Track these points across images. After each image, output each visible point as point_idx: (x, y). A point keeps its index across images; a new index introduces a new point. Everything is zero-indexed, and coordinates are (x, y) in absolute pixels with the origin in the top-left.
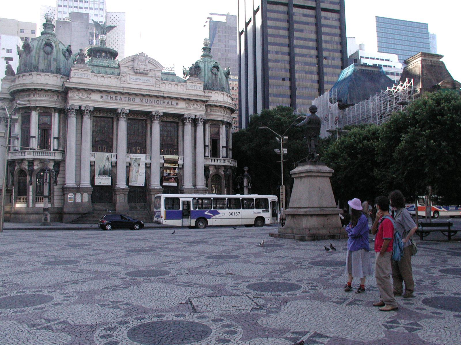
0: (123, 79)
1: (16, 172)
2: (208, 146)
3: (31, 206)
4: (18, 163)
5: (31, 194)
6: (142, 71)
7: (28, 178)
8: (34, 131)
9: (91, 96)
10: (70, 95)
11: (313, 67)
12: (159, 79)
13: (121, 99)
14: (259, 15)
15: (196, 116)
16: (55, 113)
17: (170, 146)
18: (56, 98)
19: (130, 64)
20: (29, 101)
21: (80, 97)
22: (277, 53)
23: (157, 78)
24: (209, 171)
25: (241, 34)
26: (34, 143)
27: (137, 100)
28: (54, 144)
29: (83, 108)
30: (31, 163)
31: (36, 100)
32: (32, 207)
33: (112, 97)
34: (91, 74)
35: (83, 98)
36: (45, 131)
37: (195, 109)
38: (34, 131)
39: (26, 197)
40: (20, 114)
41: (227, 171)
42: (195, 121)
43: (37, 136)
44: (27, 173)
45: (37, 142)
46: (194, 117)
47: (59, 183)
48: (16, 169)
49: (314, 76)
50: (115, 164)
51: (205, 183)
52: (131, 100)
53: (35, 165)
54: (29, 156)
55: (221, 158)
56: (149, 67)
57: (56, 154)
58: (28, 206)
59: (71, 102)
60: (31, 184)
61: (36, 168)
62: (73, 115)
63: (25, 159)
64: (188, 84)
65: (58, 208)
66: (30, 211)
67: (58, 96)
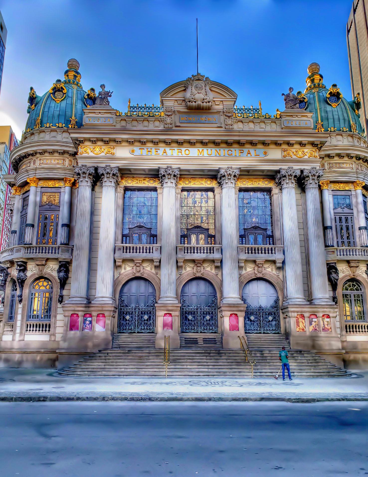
2: (331, 228)
5: (19, 317)
6: (199, 102)
9: (113, 151)
12: (230, 115)
15: (302, 171)
24: (336, 272)
29: (100, 171)
31: (36, 169)
33: (149, 150)
34: (114, 116)
45: (36, 233)
46: (298, 173)
50: (158, 264)
51: (331, 294)
59: (81, 162)
61: (29, 273)
62: (84, 183)
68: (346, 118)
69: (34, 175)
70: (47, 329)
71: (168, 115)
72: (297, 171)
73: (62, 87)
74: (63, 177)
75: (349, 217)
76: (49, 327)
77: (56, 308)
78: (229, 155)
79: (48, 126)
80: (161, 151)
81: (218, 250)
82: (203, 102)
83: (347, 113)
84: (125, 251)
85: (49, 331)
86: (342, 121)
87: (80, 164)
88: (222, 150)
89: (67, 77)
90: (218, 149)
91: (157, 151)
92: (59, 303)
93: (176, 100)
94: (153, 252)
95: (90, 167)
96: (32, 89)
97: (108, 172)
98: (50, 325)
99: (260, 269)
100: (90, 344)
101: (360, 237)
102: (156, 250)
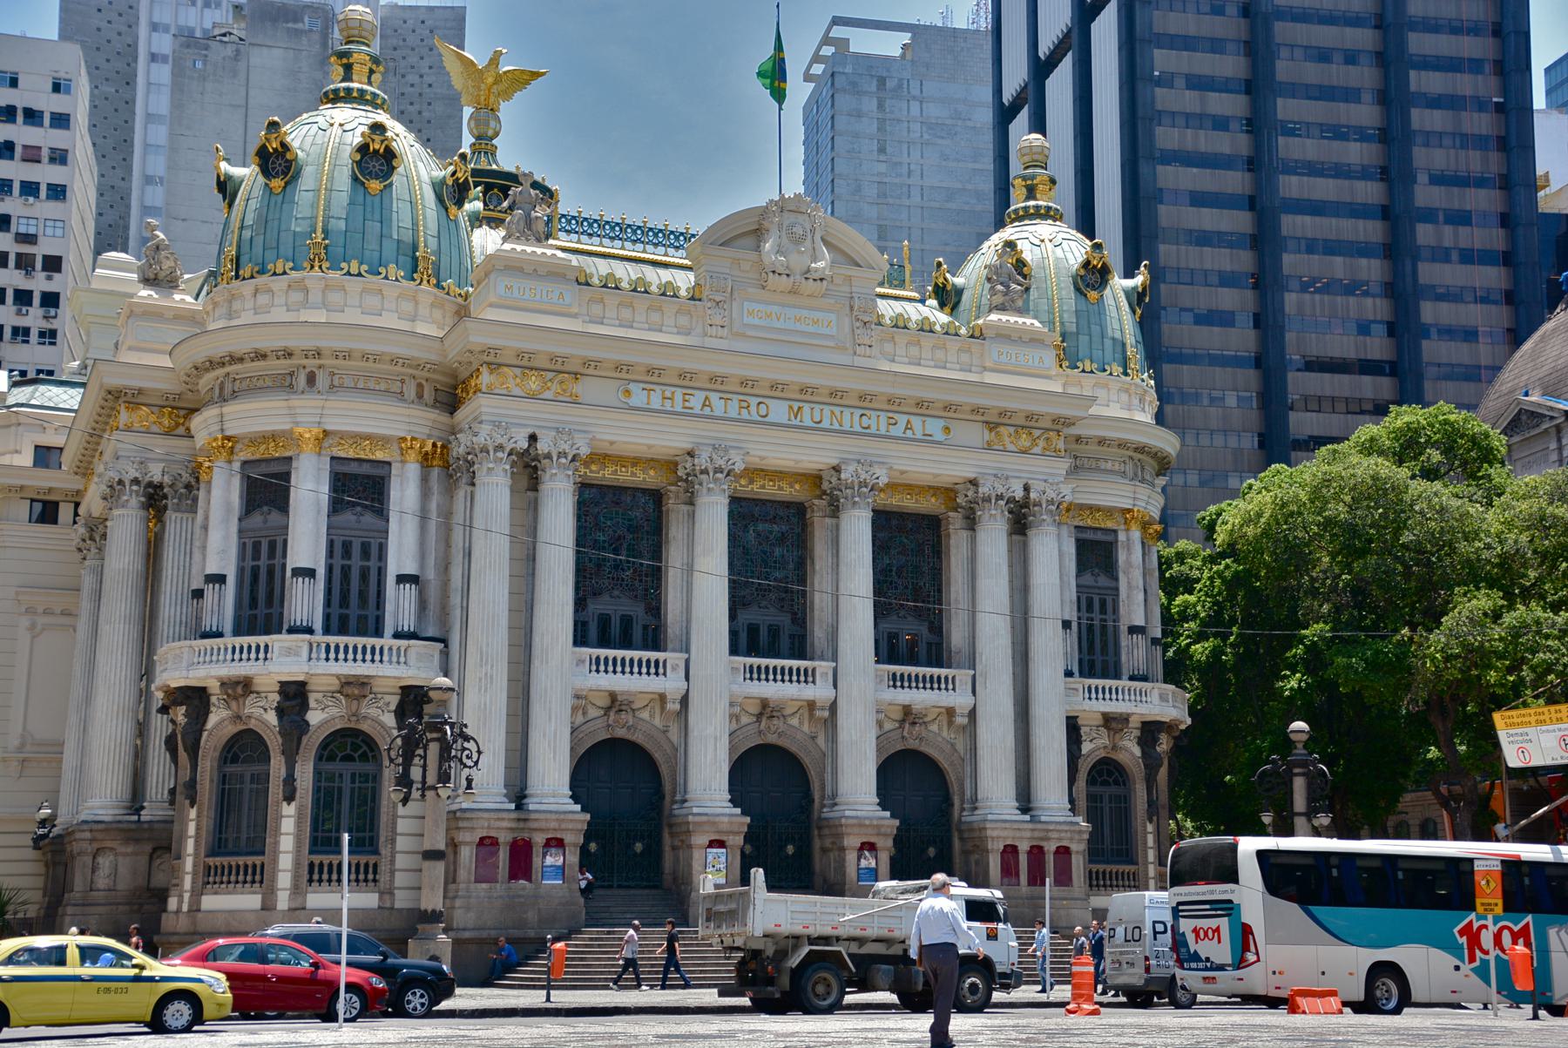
3: (283, 901)
5: (287, 843)
7: (277, 766)
9: (577, 388)
10: (485, 378)
11: (1364, 262)
13: (706, 403)
14: (1105, 30)
15: (1027, 488)
16: (403, 462)
17: (915, 624)
22: (1199, 199)
25: (1005, 115)
26: (306, 601)
28: (400, 606)
29: (542, 446)
30: (294, 696)
33: (668, 394)
35: (548, 395)
39: (258, 860)
40: (237, 466)
41: (1155, 741)
43: (321, 572)
44: (274, 742)
49: (1369, 301)
50: (677, 707)
52: (753, 408)
53: (312, 704)
54: (285, 659)
55: (1125, 677)
57: (412, 654)
60: (289, 798)
61: (314, 717)
67: (420, 386)
70: (370, 877)
75: (1109, 600)
76: (375, 872)
77: (395, 817)
79: (354, 270)
80: (696, 401)
85: (375, 881)
88: (847, 412)
90: (837, 410)
98: (375, 866)
100: (531, 916)
101: (1130, 653)
102: (674, 669)
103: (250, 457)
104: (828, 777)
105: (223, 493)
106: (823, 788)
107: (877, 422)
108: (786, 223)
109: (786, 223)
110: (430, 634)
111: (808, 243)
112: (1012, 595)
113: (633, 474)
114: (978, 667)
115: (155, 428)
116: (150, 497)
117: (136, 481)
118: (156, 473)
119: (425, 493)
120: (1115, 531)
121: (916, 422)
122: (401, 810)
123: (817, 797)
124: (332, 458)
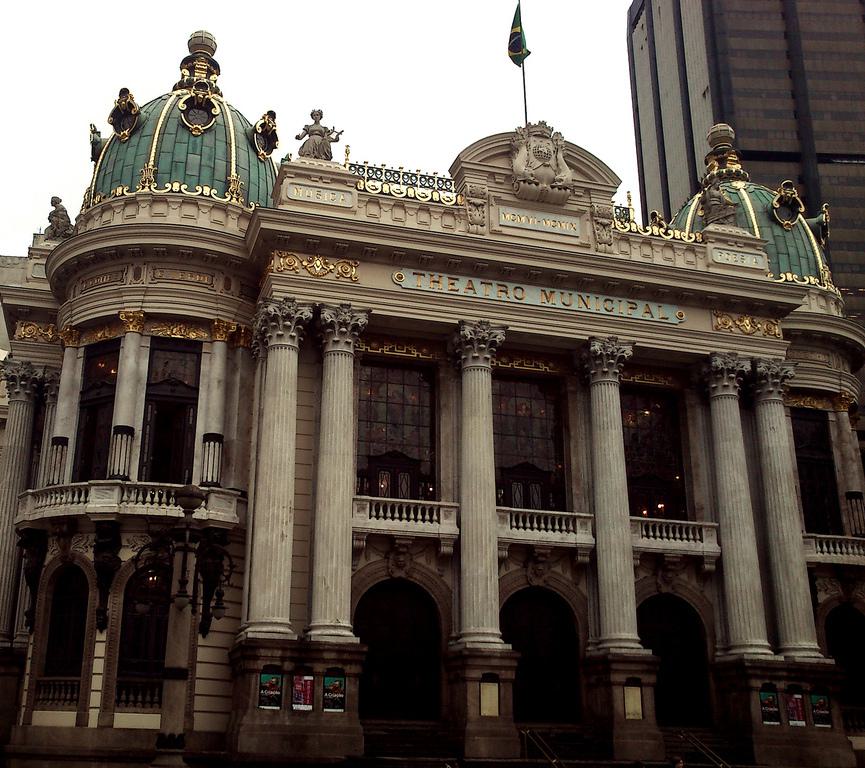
0: (477, 215)
1: (45, 576)
4: (61, 535)
5: (98, 666)
6: (544, 185)
7: (93, 596)
8: (129, 407)
10: (278, 262)
12: (606, 221)
17: (663, 483)
18: (219, 285)
19: (501, 163)
20: (119, 293)
21: (318, 276)
23: (601, 220)
26: (126, 458)
27: (533, 296)
28: (205, 464)
29: (327, 315)
31: (146, 291)
32: (100, 727)
33: (436, 278)
36: (171, 408)
37: (747, 339)
38: (129, 407)
42: (751, 390)
43: (138, 432)
44: (91, 577)
45: (137, 451)
47: (216, 624)
48: (46, 563)
52: (511, 293)
53: (124, 542)
54: (102, 502)
56: (567, 175)
58: (82, 721)
59: (279, 291)
60: (102, 627)
61: (126, 555)
63: (86, 516)
64: (710, 246)
65: (207, 733)
66: (91, 743)
68: (810, 254)
69: (140, 304)
71: (474, 204)
72: (743, 363)
73: (209, 99)
74: (212, 317)
78: (516, 298)
81: (584, 524)
82: (553, 187)
83: (811, 244)
84: (374, 513)
86: (803, 262)
87: (278, 296)
88: (593, 297)
89: (187, 73)
90: (584, 295)
91: (452, 284)
92: (200, 637)
93: (492, 175)
94: (438, 521)
95: (304, 305)
96: (124, 92)
97: (345, 320)
99: (670, 575)
103: (93, 341)
104: (591, 619)
105: (71, 373)
106: (587, 629)
107: (621, 308)
108: (533, 145)
109: (533, 145)
110: (232, 486)
111: (552, 162)
112: (746, 463)
113: (408, 352)
114: (723, 521)
115: (41, 339)
116: (36, 390)
117: (23, 378)
118: (40, 373)
119: (230, 366)
120: (824, 414)
121: (654, 307)
122: (201, 641)
123: (581, 638)
124: (153, 338)
